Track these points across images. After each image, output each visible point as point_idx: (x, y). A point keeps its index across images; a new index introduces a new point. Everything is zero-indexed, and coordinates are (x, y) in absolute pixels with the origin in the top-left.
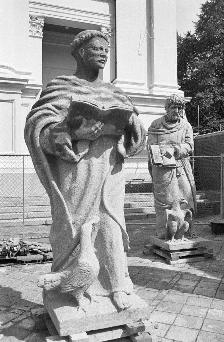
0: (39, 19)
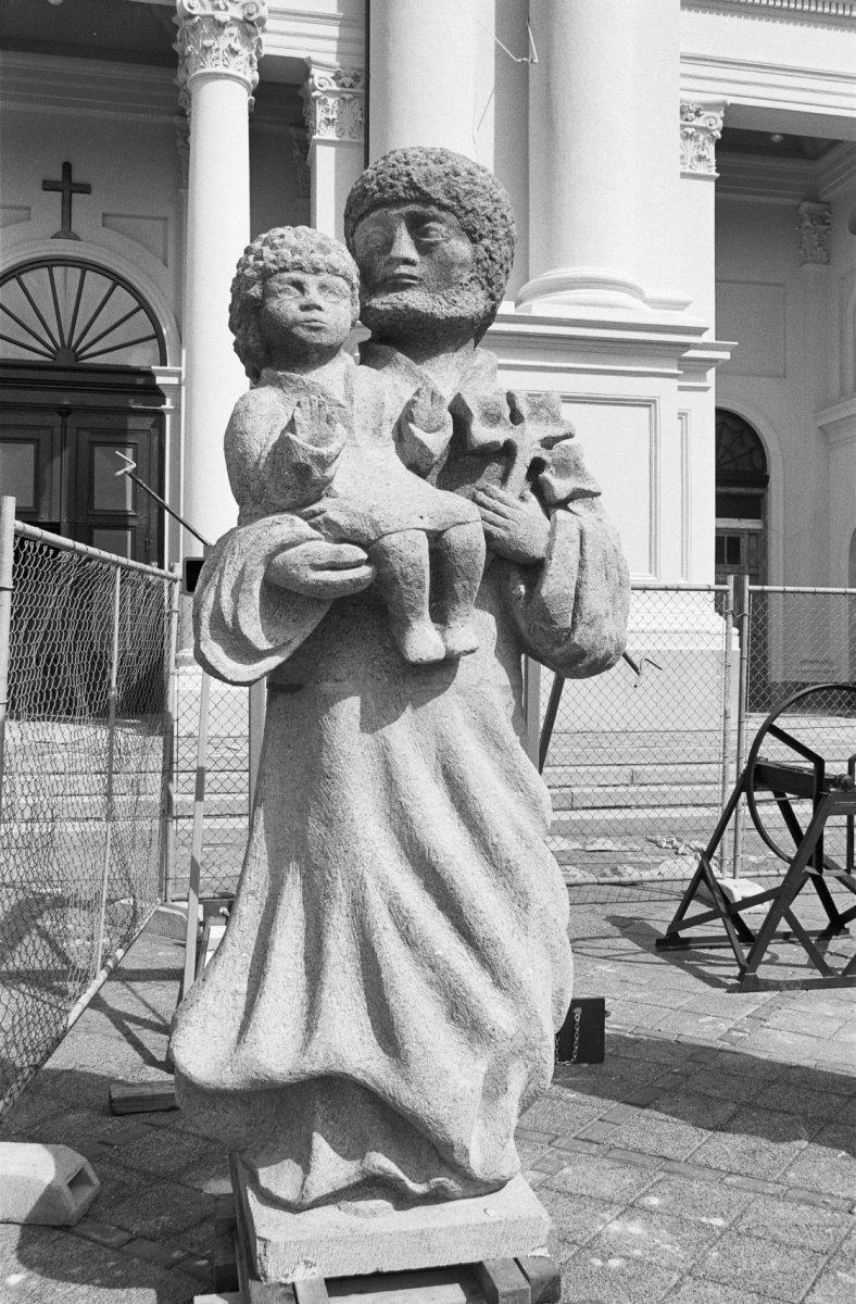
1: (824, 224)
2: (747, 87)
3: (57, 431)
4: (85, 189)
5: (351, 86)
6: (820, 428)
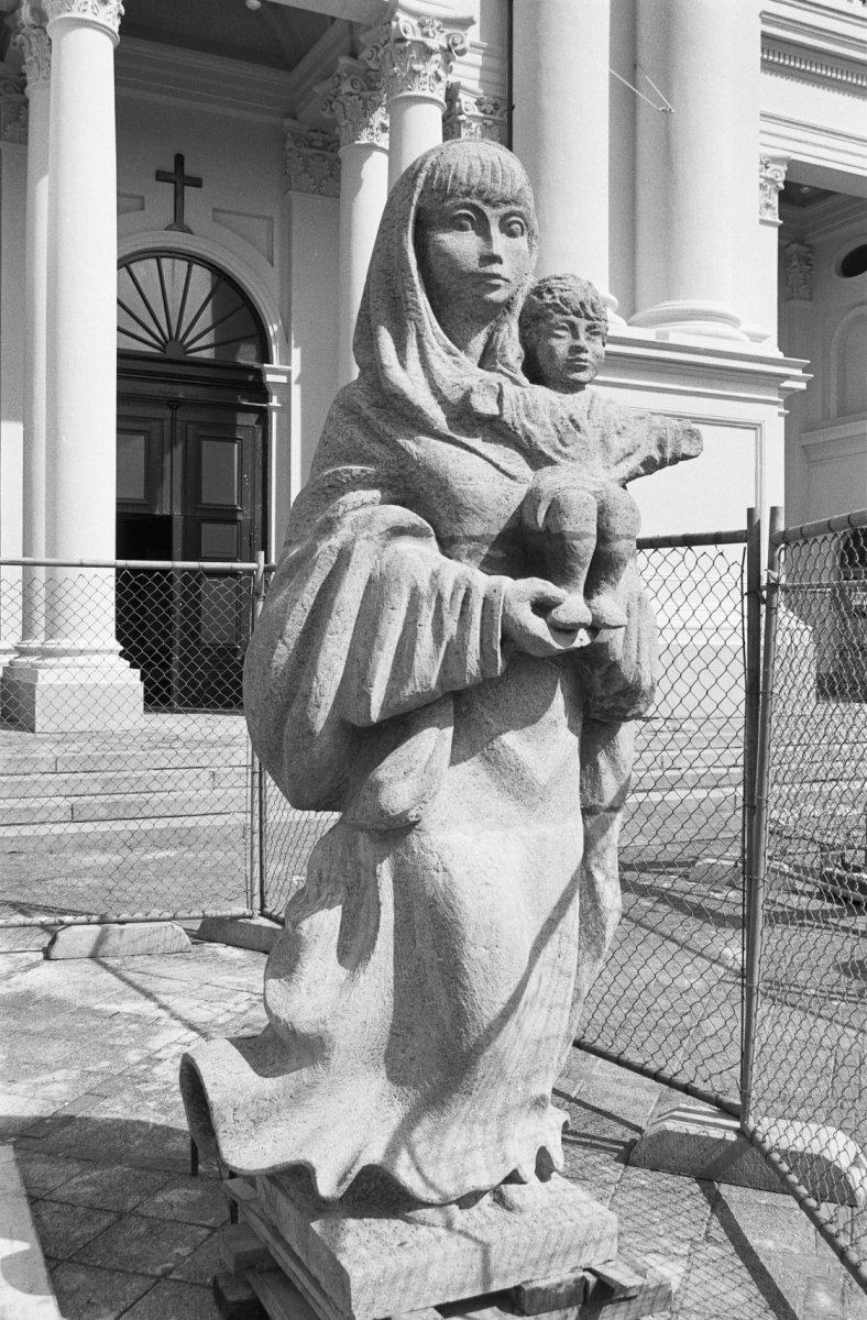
0: (772, 166)
3: (167, 423)
4: (197, 183)
5: (491, 113)
6: (803, 447)
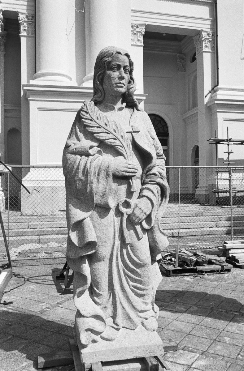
0: (140, 27)
1: (183, 60)
2: (179, 22)
5: (31, 19)
6: (184, 119)
